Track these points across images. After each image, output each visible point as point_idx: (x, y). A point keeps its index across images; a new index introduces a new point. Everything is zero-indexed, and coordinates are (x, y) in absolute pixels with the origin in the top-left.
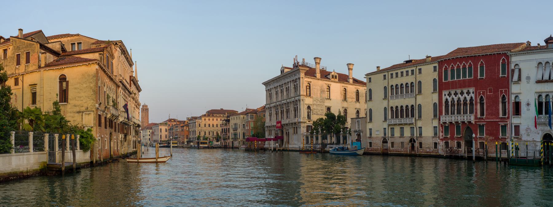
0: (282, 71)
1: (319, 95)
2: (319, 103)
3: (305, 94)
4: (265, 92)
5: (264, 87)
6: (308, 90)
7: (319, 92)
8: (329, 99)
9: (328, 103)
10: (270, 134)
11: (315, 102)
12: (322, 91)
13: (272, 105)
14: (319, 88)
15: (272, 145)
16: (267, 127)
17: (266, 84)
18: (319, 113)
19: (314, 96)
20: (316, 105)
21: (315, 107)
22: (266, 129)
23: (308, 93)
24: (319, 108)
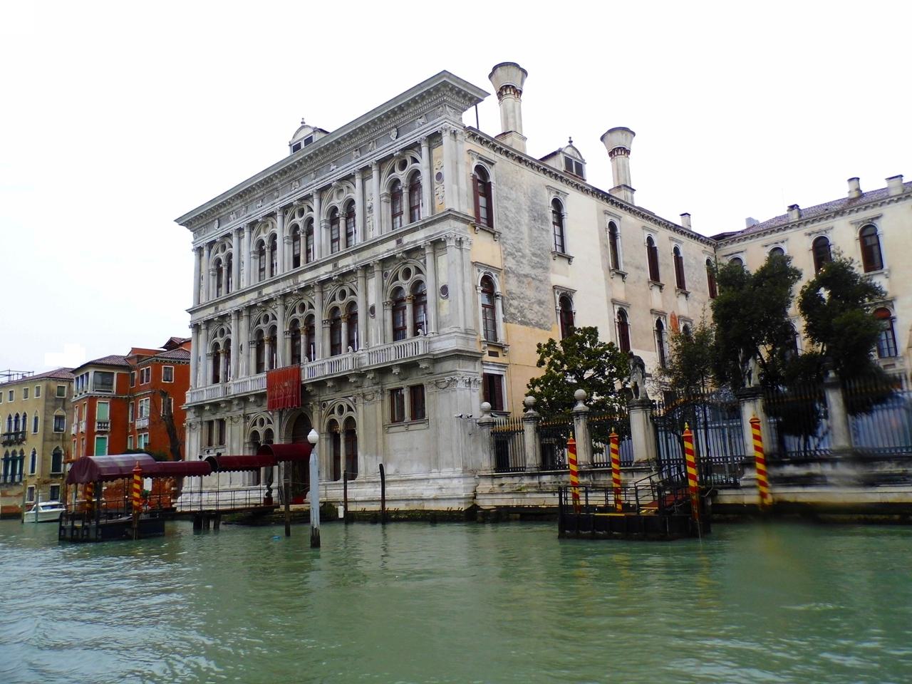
0: (296, 148)
1: (525, 229)
2: (526, 269)
3: (471, 213)
4: (192, 257)
5: (187, 235)
6: (482, 201)
7: (525, 218)
8: (562, 254)
9: (561, 276)
10: (214, 431)
11: (511, 263)
12: (538, 217)
13: (229, 307)
14: (523, 199)
15: (234, 490)
16: (199, 408)
17: (194, 221)
18: (530, 316)
19: (505, 232)
20: (518, 276)
21: (513, 285)
22: (190, 417)
23: (483, 213)
24: (530, 293)
